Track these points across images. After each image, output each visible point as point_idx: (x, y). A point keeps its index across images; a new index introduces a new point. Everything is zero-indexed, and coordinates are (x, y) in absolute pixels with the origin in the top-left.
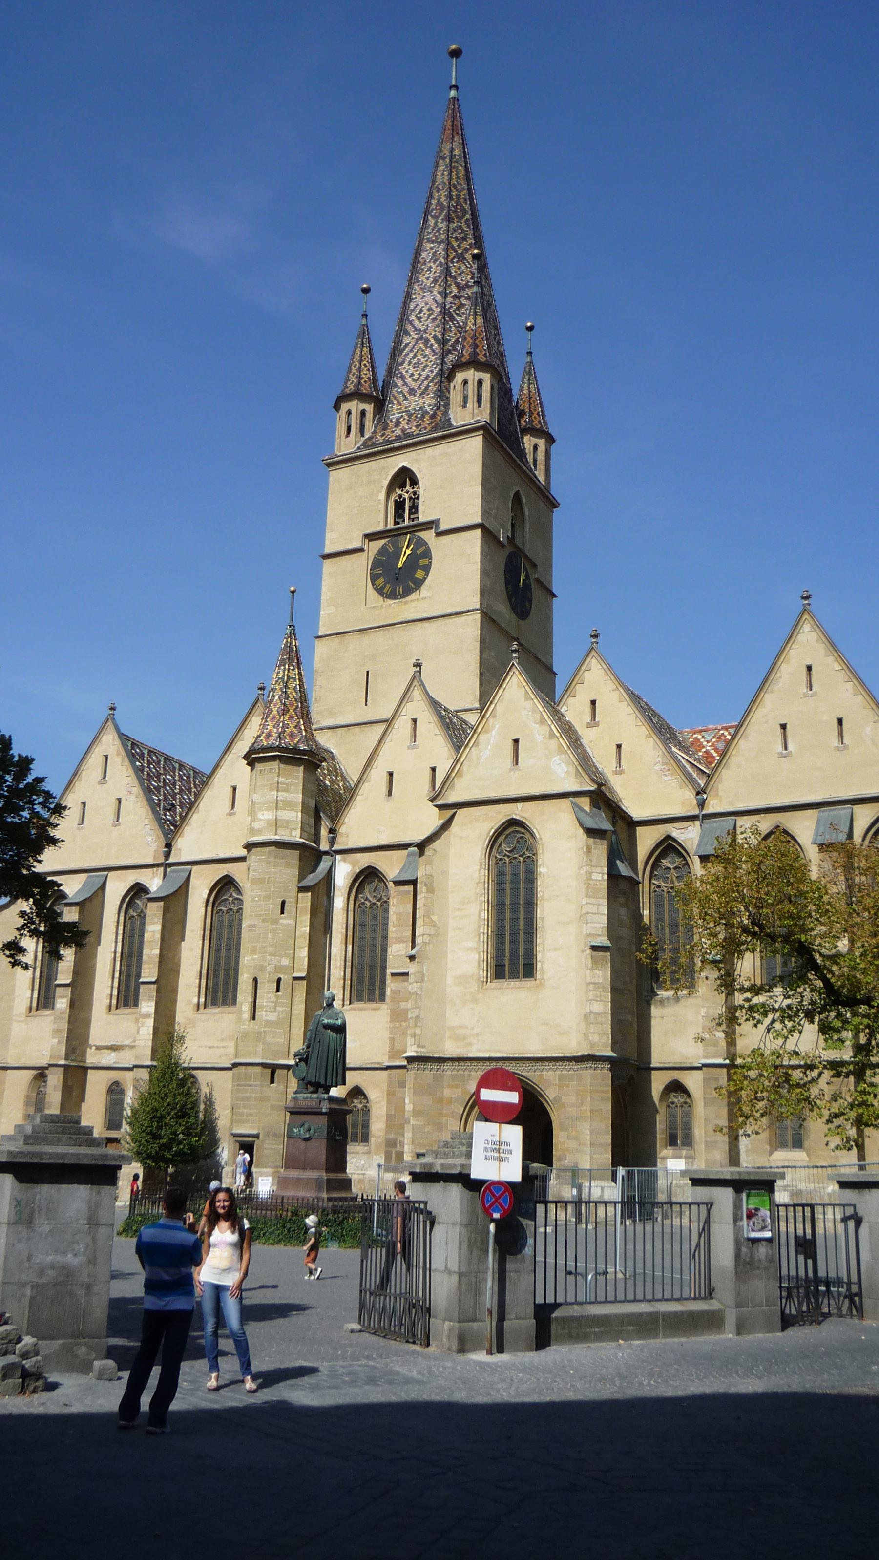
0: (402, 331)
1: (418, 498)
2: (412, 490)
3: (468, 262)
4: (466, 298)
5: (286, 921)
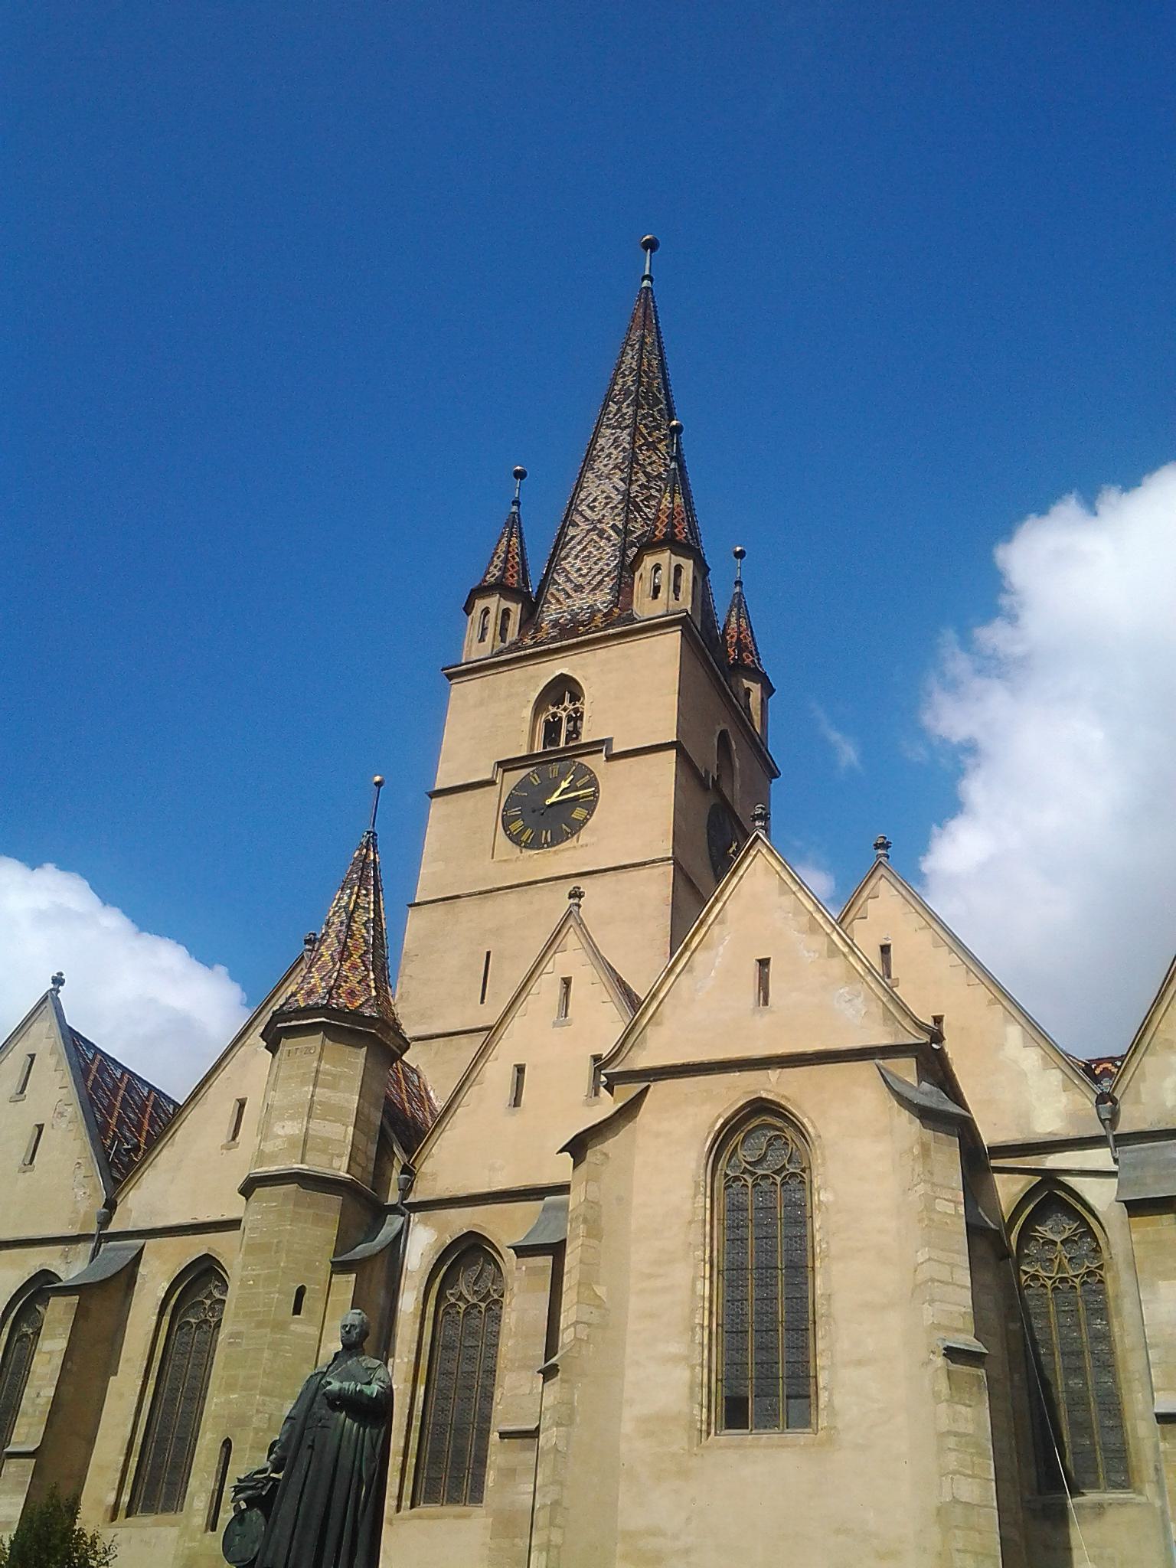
0: (567, 522)
1: (581, 718)
2: (571, 707)
4: (657, 490)
5: (302, 1328)
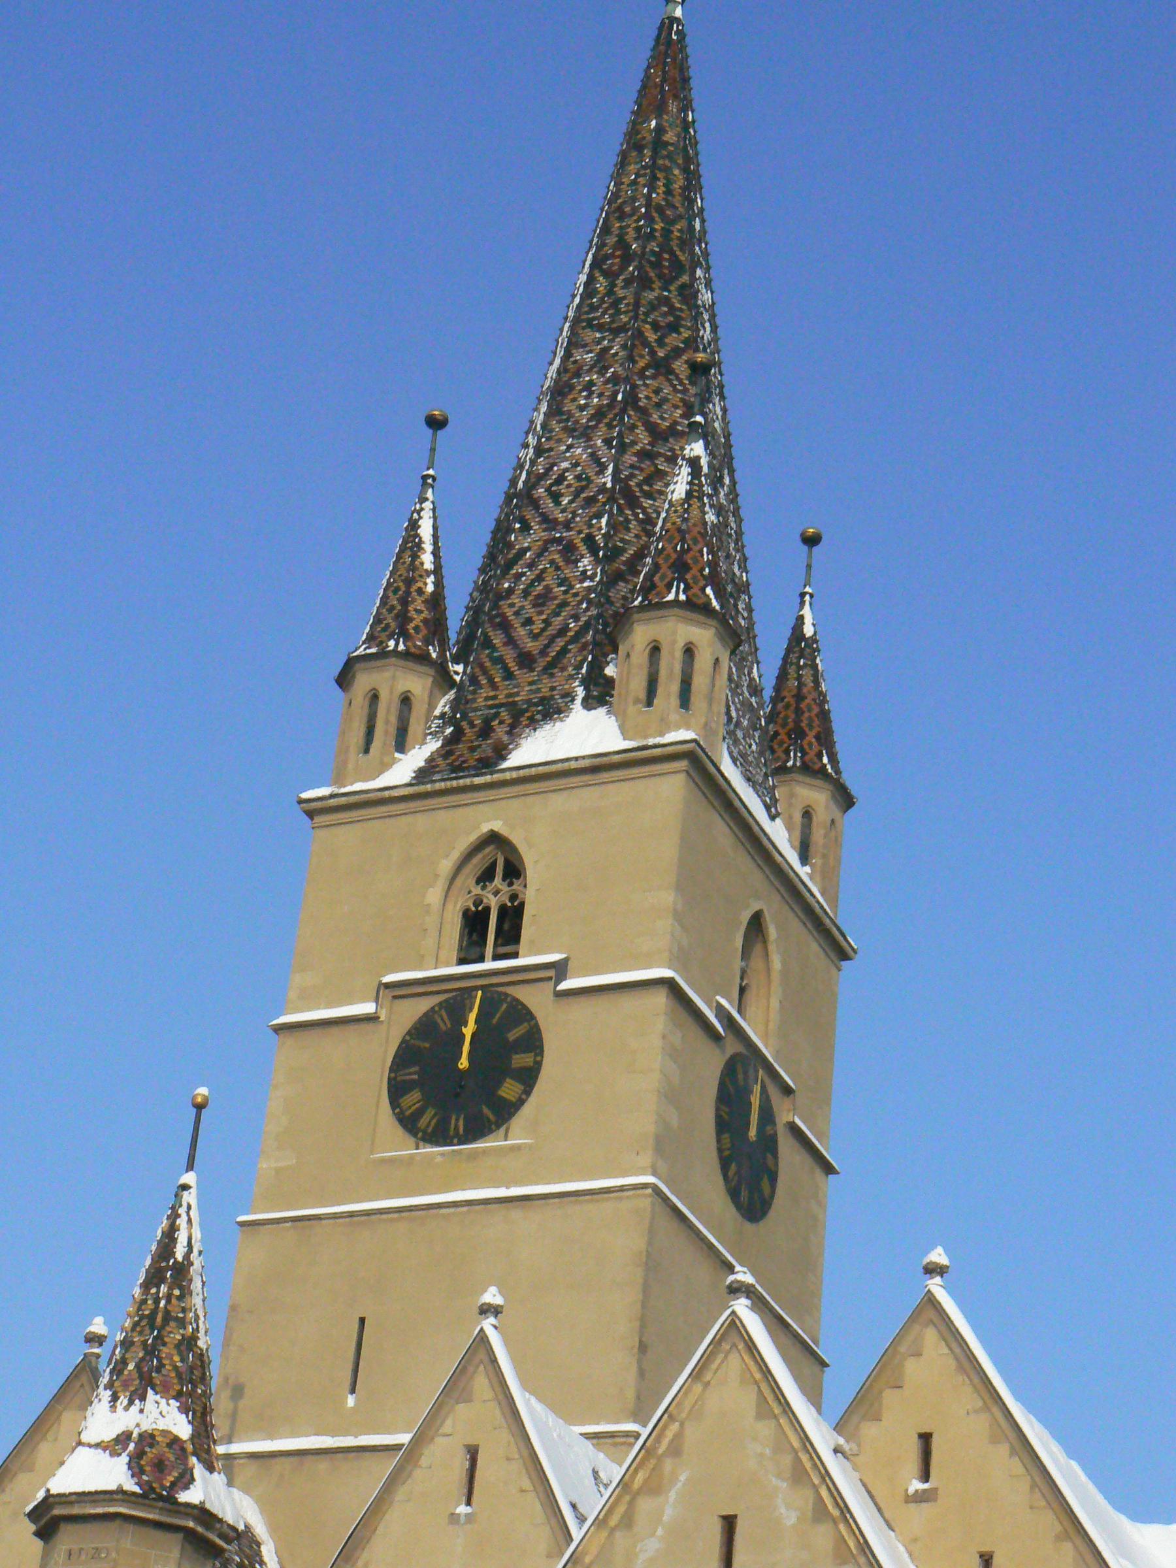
3: (678, 378)
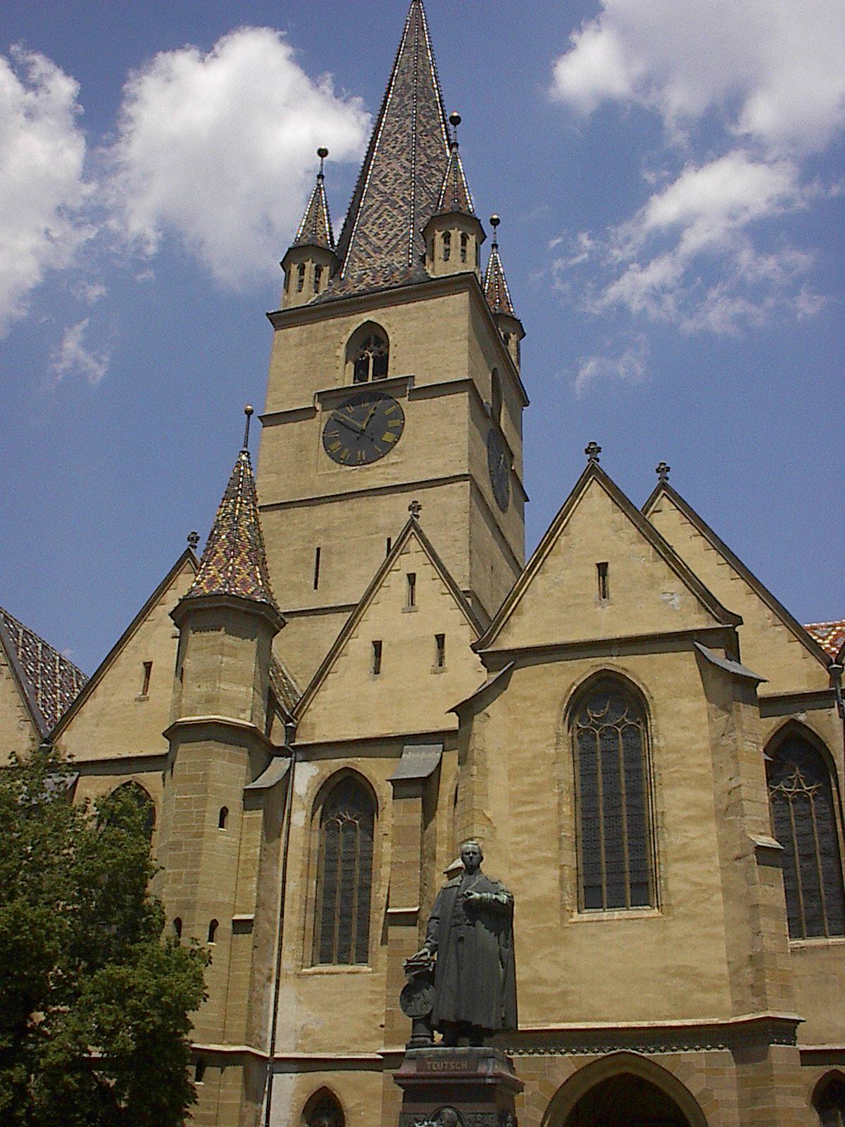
5: (226, 838)
